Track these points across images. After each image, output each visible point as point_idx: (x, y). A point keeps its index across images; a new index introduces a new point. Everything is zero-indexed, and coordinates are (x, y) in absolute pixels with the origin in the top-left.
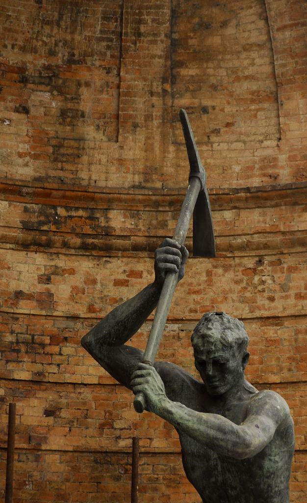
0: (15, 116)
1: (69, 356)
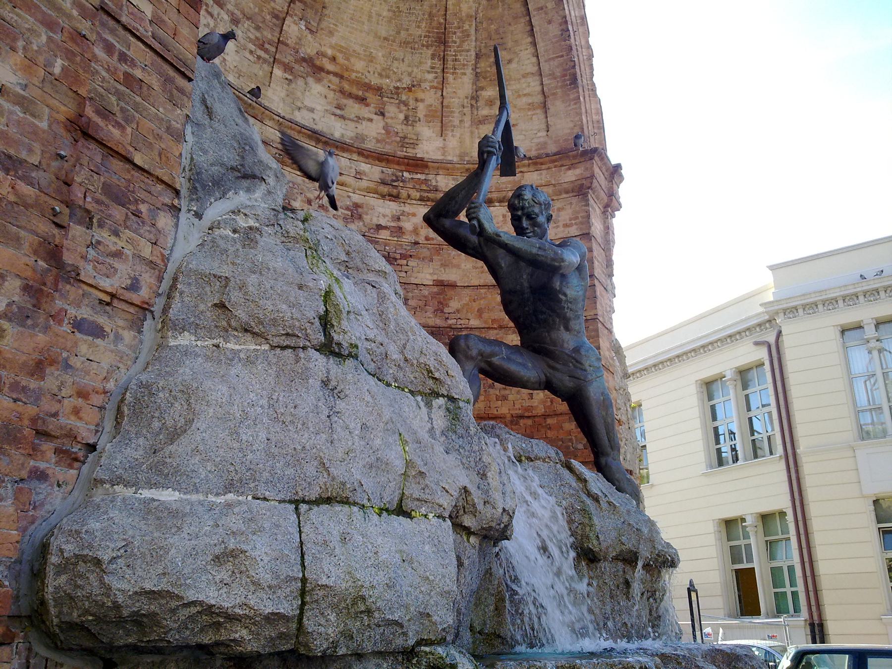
0: (375, 117)
1: (413, 267)
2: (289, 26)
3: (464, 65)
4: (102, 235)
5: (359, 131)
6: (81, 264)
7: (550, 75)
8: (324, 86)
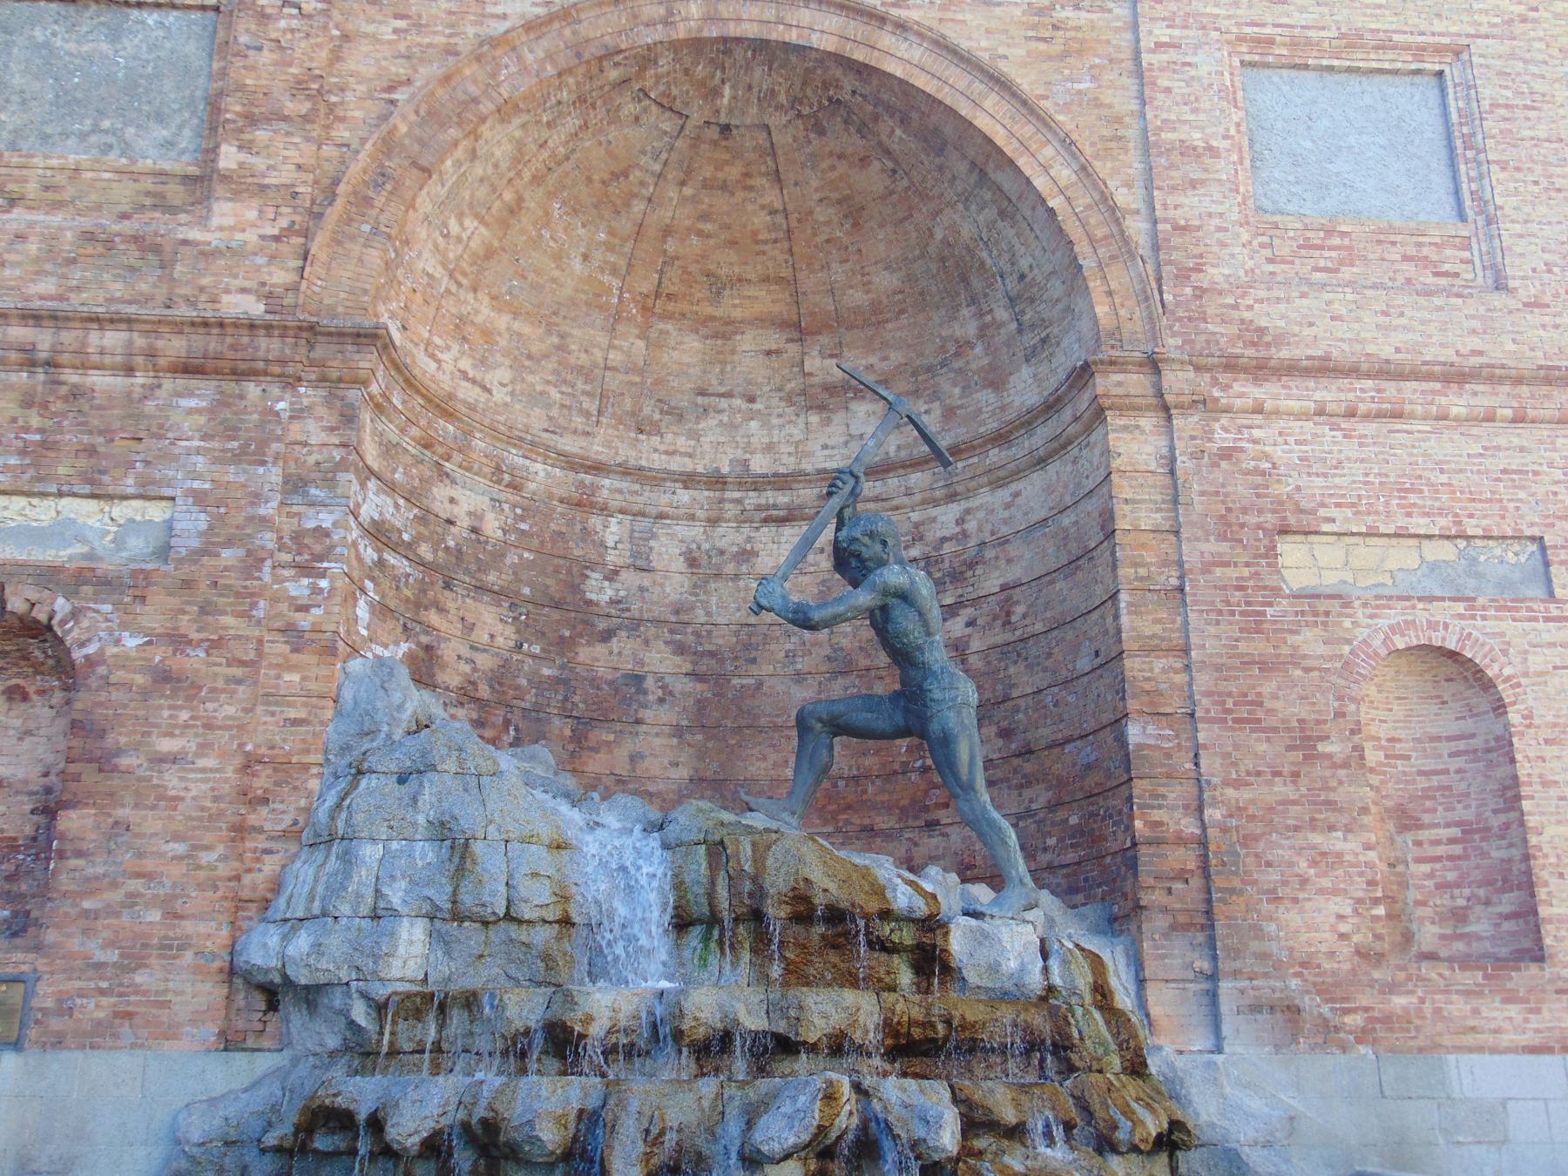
4: (276, 806)
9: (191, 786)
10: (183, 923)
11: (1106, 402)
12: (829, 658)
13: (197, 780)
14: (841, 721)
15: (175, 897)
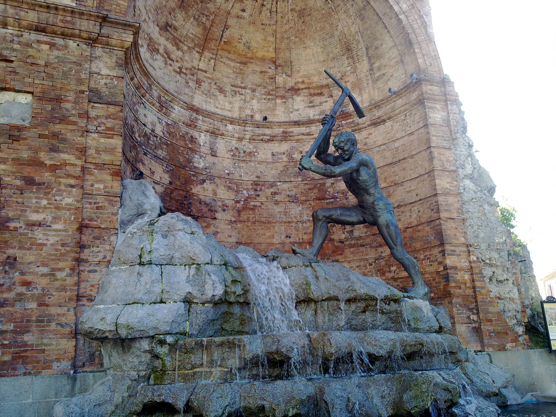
0: (328, 99)
2: (278, 79)
3: (362, 56)
5: (321, 109)
6: (88, 258)
7: (400, 44)
8: (302, 96)
9: (50, 238)
10: (49, 308)
11: (426, 96)
12: (289, 196)
13: (53, 236)
14: (334, 217)
15: (44, 295)
